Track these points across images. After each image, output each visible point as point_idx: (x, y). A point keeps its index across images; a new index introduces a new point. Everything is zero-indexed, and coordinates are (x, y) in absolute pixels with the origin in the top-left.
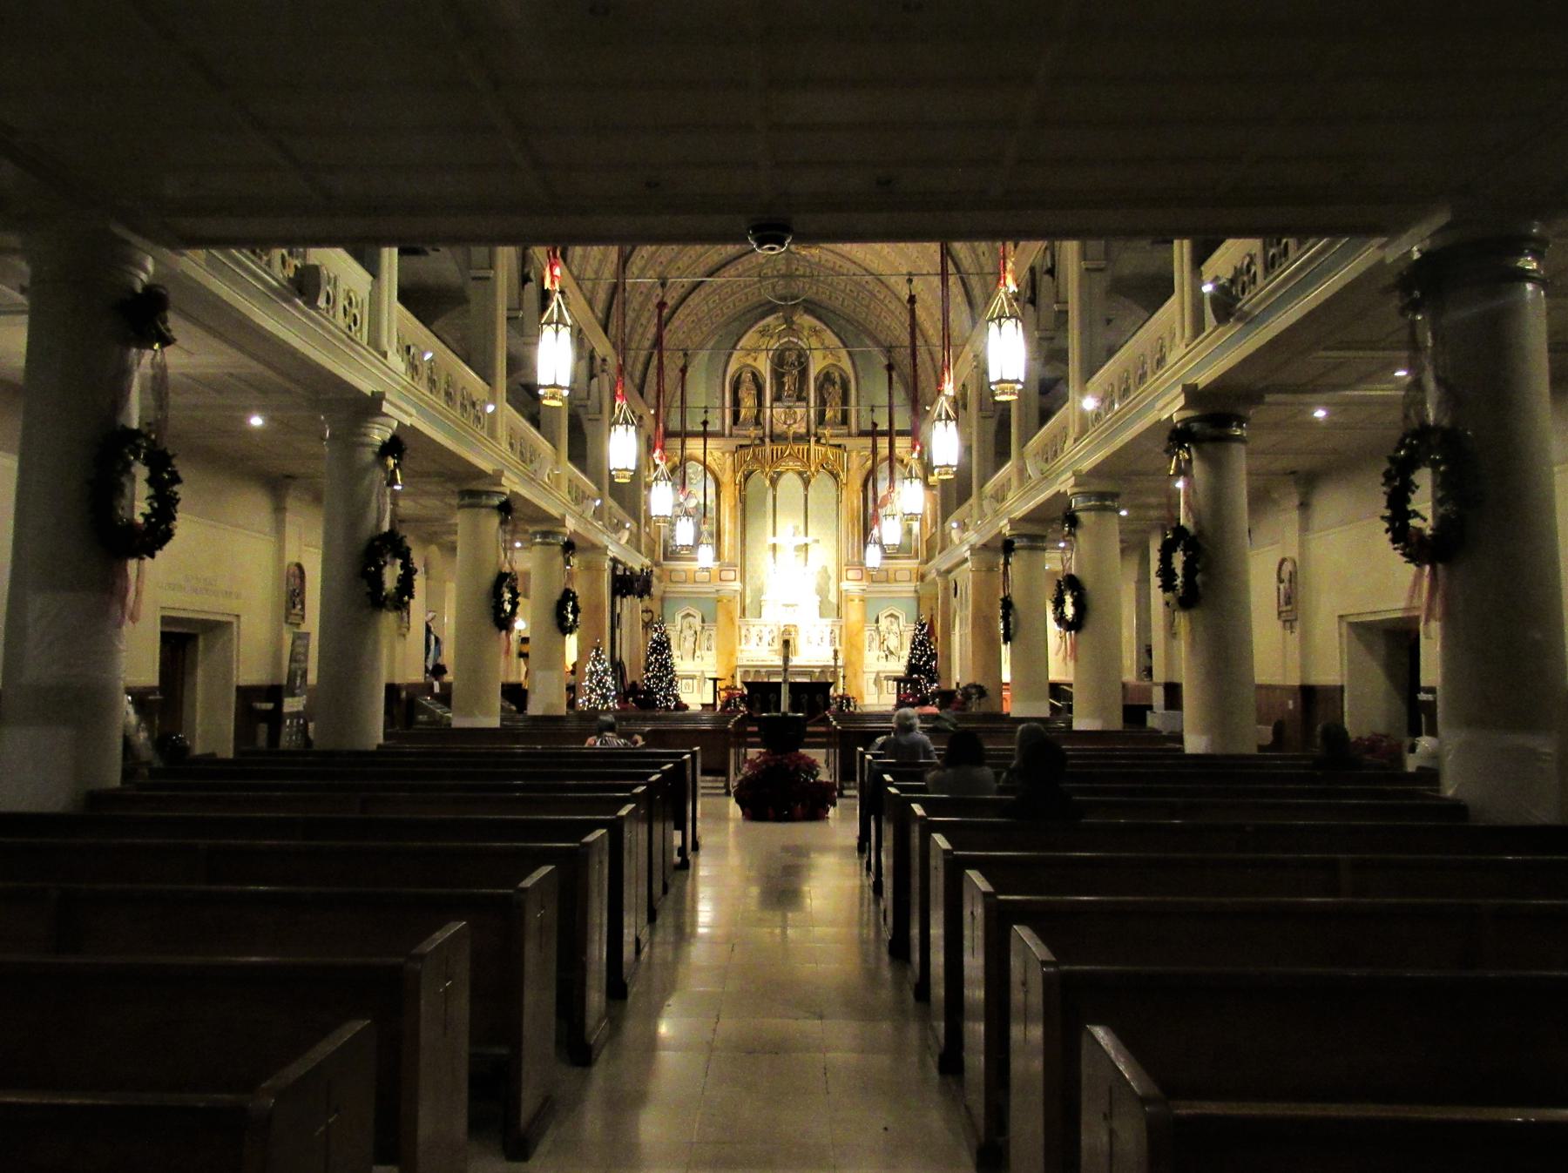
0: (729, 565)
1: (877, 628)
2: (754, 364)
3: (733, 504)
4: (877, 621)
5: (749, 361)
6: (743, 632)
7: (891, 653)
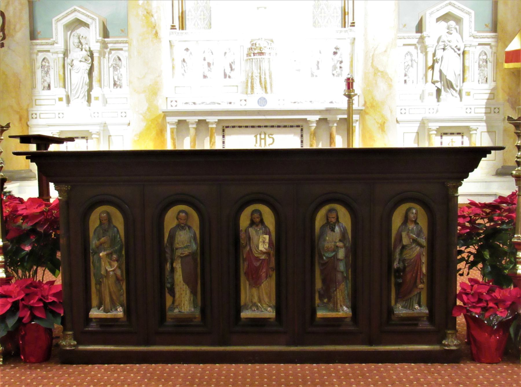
1: (422, 38)
6: (179, 53)
7: (450, 85)
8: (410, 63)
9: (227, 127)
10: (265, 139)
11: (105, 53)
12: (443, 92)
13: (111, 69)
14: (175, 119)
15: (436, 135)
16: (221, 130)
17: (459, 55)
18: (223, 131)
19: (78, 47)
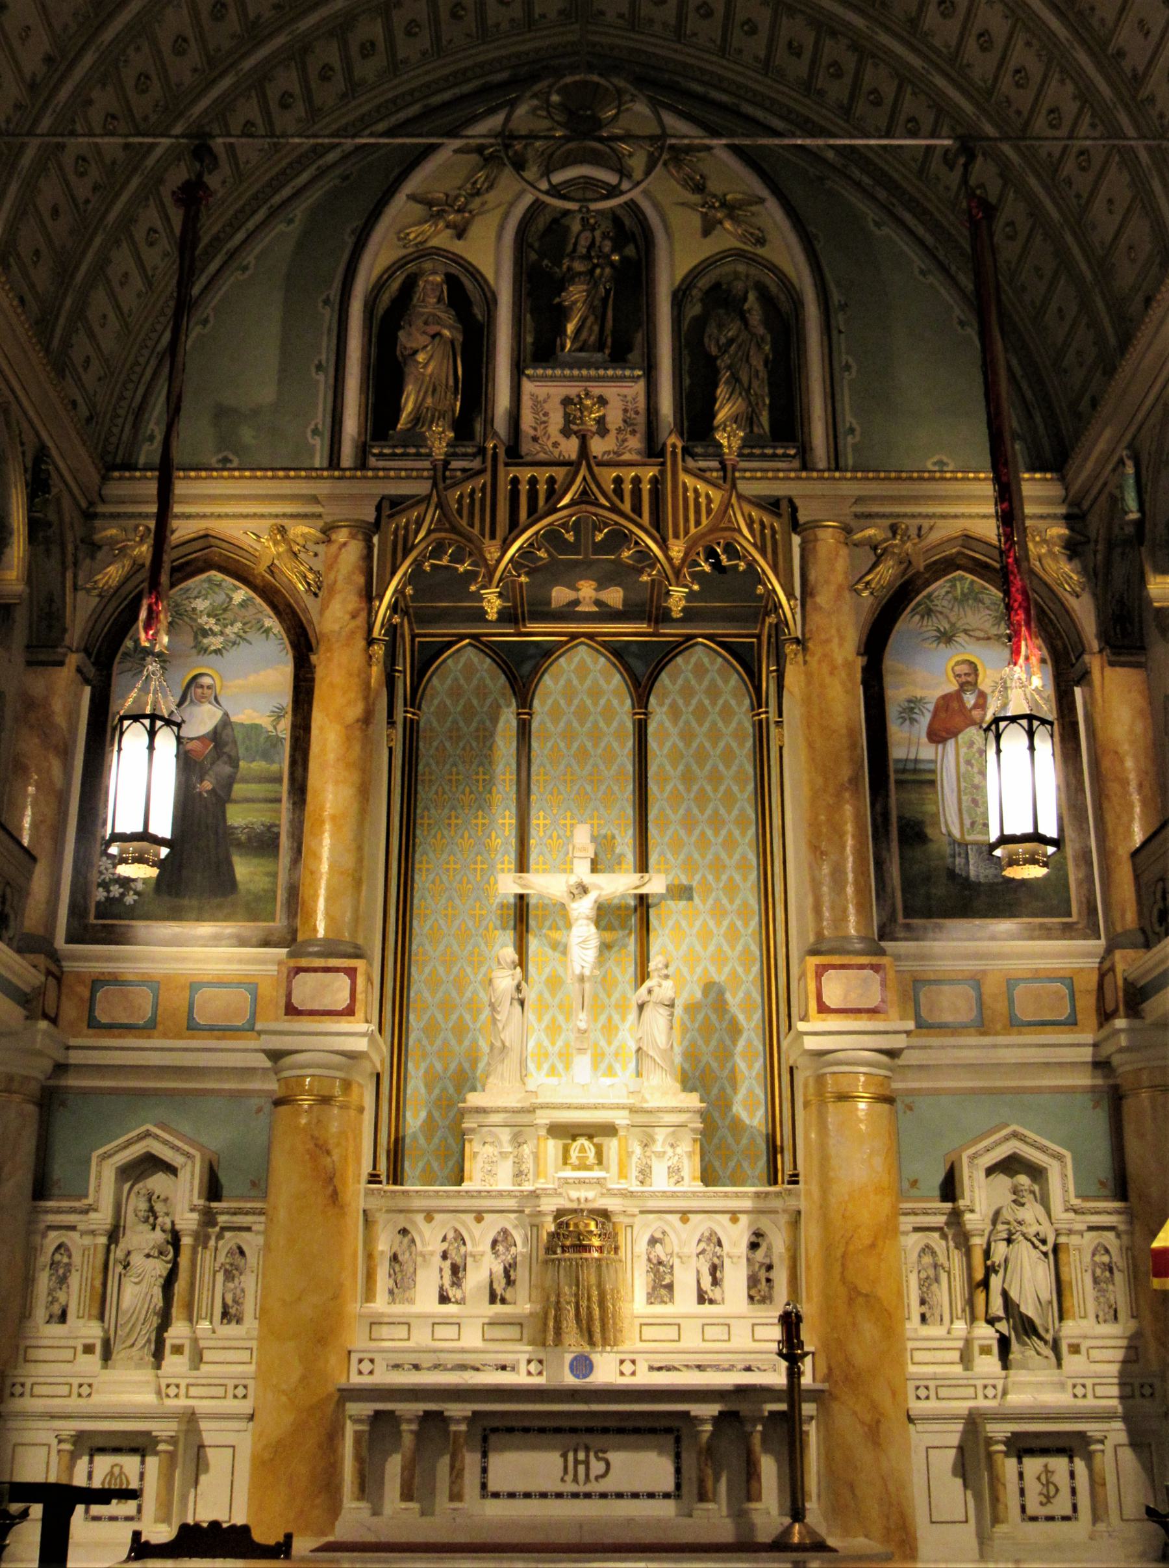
0: (331, 948)
1: (956, 1217)
2: (458, 247)
3: (356, 711)
4: (949, 1189)
5: (442, 239)
7: (1027, 1328)
8: (931, 1272)
9: (495, 1430)
10: (587, 1463)
11: (207, 1237)
12: (1015, 1346)
13: (220, 1277)
14: (366, 1409)
15: (1007, 1454)
16: (479, 1438)
17: (1045, 1254)
18: (485, 1439)
19: (146, 1221)
